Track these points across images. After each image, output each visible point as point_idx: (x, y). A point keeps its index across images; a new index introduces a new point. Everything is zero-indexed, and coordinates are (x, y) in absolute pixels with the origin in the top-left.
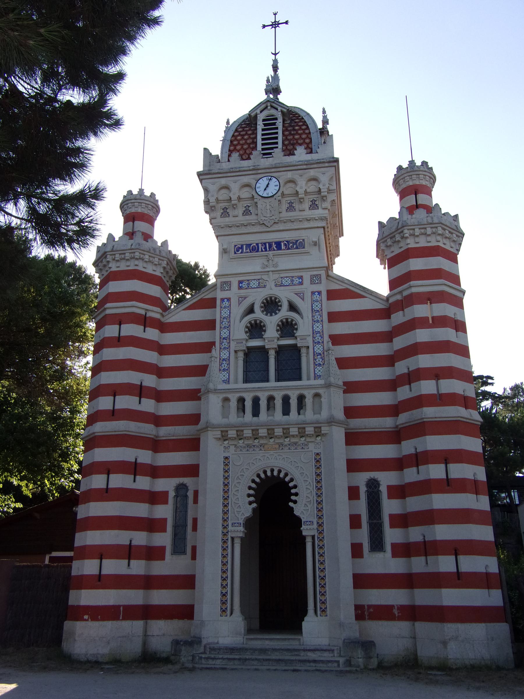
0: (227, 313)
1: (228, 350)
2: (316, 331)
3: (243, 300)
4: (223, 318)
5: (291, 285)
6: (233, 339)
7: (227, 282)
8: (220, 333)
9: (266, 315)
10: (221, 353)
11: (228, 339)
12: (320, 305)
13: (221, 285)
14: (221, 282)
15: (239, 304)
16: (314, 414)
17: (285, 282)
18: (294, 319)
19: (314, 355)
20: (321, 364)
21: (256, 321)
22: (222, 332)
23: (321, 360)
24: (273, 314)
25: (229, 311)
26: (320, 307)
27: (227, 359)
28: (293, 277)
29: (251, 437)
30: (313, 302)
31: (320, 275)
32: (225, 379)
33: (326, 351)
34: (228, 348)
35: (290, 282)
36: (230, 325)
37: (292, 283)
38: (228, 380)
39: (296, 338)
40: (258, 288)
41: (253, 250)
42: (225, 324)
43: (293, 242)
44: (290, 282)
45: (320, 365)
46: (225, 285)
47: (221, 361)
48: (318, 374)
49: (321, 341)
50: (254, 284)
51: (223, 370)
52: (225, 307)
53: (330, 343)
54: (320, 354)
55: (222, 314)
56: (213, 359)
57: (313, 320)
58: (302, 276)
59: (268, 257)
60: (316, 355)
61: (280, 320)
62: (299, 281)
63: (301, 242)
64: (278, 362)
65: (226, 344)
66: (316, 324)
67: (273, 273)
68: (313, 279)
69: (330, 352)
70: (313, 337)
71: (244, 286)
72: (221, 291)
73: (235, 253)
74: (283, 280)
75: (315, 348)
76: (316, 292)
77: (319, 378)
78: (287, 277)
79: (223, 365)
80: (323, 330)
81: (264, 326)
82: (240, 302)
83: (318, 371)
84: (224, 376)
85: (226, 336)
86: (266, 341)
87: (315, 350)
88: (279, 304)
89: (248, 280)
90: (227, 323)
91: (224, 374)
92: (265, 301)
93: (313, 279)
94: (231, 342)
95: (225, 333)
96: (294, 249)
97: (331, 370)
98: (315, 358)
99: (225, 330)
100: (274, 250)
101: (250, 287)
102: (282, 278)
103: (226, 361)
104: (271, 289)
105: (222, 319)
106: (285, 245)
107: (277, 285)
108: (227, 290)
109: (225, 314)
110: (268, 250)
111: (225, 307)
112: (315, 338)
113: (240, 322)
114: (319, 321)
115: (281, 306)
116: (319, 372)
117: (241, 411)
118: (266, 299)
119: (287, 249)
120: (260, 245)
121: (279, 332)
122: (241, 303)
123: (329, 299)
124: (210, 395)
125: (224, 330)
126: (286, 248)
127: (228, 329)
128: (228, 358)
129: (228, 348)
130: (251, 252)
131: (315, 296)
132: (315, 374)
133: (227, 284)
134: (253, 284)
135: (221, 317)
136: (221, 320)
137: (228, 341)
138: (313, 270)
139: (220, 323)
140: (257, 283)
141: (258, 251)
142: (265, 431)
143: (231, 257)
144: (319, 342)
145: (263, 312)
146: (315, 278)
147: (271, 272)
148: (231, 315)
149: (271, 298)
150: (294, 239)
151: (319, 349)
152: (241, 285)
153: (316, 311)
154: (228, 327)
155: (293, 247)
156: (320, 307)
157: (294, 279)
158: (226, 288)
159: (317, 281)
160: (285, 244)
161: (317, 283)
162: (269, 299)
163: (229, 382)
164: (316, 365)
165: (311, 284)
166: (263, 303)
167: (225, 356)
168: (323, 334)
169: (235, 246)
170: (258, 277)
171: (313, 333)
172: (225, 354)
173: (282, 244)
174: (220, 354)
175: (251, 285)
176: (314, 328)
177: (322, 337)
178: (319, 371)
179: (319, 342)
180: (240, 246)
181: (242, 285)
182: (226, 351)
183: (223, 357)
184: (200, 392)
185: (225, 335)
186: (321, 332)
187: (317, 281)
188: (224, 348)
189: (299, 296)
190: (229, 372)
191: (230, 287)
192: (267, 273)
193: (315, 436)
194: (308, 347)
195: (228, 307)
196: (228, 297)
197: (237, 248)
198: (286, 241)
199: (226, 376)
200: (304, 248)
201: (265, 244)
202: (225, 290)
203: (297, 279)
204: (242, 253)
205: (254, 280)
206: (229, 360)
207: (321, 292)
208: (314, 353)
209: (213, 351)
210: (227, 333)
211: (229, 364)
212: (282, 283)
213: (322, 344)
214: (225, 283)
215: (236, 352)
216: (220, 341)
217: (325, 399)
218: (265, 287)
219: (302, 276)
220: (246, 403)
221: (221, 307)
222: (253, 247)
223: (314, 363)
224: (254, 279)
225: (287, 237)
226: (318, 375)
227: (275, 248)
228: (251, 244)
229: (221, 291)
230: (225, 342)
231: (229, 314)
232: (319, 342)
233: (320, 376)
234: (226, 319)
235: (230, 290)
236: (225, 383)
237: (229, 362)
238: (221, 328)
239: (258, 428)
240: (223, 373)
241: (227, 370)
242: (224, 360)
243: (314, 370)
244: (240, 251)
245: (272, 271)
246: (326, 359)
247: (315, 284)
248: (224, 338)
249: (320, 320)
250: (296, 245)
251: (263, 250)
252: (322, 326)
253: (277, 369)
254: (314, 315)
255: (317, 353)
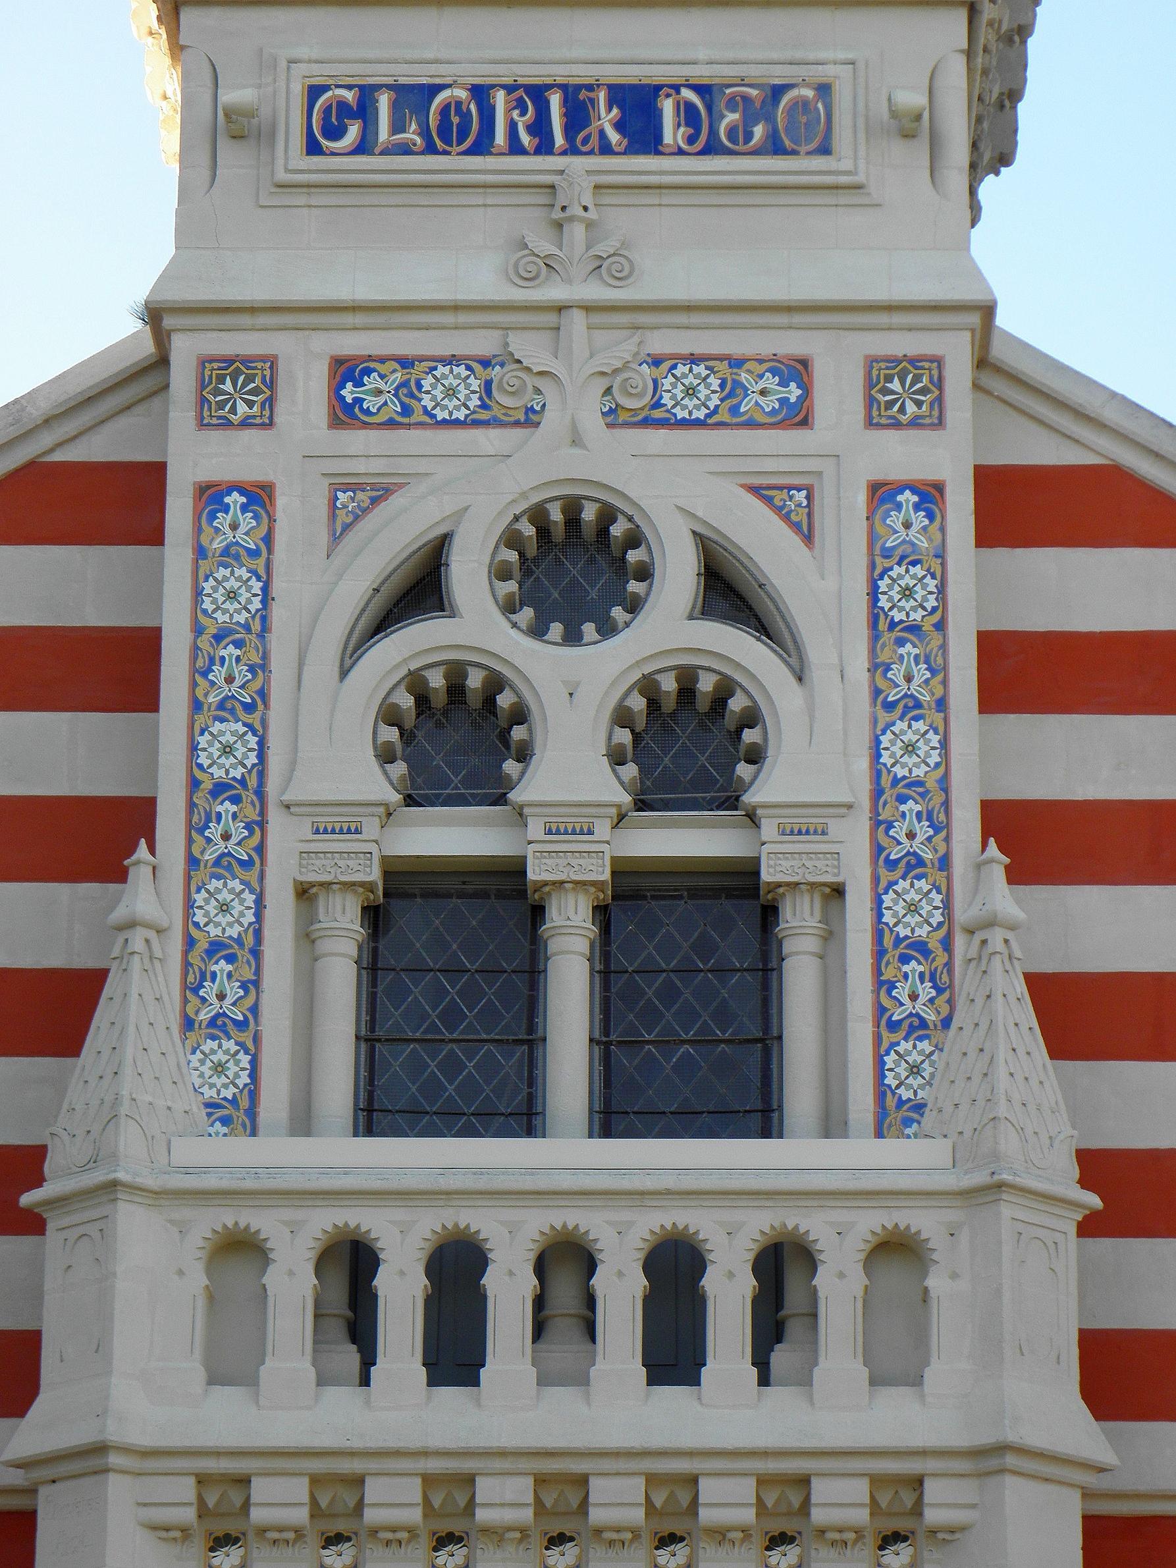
0: (244, 596)
1: (252, 875)
2: (896, 781)
3: (366, 511)
4: (218, 638)
5: (721, 425)
6: (286, 797)
7: (247, 361)
8: (193, 748)
9: (538, 631)
10: (199, 898)
11: (248, 796)
12: (932, 584)
13: (202, 386)
14: (203, 362)
15: (336, 538)
16: (874, 1382)
17: (679, 392)
18: (738, 677)
19: (879, 953)
20: (923, 1024)
21: (456, 673)
22: (203, 741)
23: (926, 991)
24: (589, 630)
25: (257, 586)
26: (931, 602)
27: (239, 941)
28: (737, 363)
29: (412, 1532)
30: (881, 563)
31: (938, 361)
32: (228, 1093)
33: (971, 933)
34: (246, 864)
35: (715, 401)
36: (263, 694)
37: (734, 410)
38: (244, 1103)
39: (752, 818)
40: (477, 423)
41: (447, 141)
42: (230, 680)
43: (746, 99)
44: (715, 401)
45: (918, 1027)
46: (228, 386)
47: (195, 958)
48: (906, 1094)
49: (928, 855)
50: (451, 392)
51: (212, 1023)
52: (230, 555)
53: (998, 874)
54: (921, 948)
55: (208, 605)
56: (138, 944)
57: (876, 692)
58: (805, 363)
59: (561, 200)
60: (892, 955)
61: (636, 675)
62: (782, 392)
63: (803, 105)
64: (606, 986)
65: (238, 831)
66: (900, 726)
67: (597, 318)
68: (886, 391)
69: (996, 937)
70: (876, 823)
71: (371, 403)
72: (202, 424)
73: (313, 148)
74: (667, 383)
75: (888, 899)
76: (902, 487)
77: (907, 1122)
78: (694, 359)
79: (209, 990)
80: (946, 776)
81: (520, 715)
82: (343, 518)
83: (902, 1071)
84: (220, 1068)
85: (237, 773)
86: (535, 829)
87: (888, 918)
88: (633, 556)
89: (406, 363)
90: (241, 673)
91: (220, 1056)
92: (529, 530)
93: (886, 391)
94: (275, 817)
95: (227, 750)
96: (755, 152)
97: (1002, 1072)
98: (888, 974)
99: (229, 730)
100: (606, 149)
101: (418, 416)
102: (656, 362)
103: (230, 959)
104: (576, 441)
105: (204, 642)
106: (689, 115)
107: (623, 417)
108: (245, 423)
109: (231, 606)
110: (559, 140)
111: (230, 555)
112: (890, 826)
113: (344, 673)
114: (918, 705)
115: (644, 573)
116: (915, 1082)
117: (337, 1329)
118: (538, 515)
119: (705, 151)
120: (500, 99)
121: (630, 771)
122: (347, 527)
123: (987, 536)
124: (121, 1206)
125: (217, 727)
126: (691, 140)
127: (255, 719)
128: (249, 940)
129: (246, 864)
130: (431, 149)
131: (896, 520)
132: (881, 1091)
133: (250, 379)
134: (438, 393)
135: (198, 630)
136: (195, 649)
137: (252, 814)
138: (883, 319)
139: (194, 670)
140: (475, 384)
141: (481, 147)
142: (521, 1489)
143: (282, 176)
144: (921, 862)
145: (510, 607)
146: (896, 385)
147: (577, 321)
148: (278, 613)
149: (572, 507)
150: (753, 71)
151: (913, 908)
152: (349, 392)
153: (897, 634)
154: (249, 708)
155: (749, 136)
156: (931, 602)
157: (744, 377)
158: (242, 408)
159: (911, 408)
160: (690, 107)
161: (915, 423)
162: (556, 515)
163: (252, 1113)
164: (893, 1026)
165: (870, 423)
166: (512, 539)
167: (224, 919)
168: (946, 804)
169: (314, 92)
170: (483, 344)
171: (877, 793)
172: (224, 908)
173: (667, 107)
174: (189, 905)
175: (427, 401)
176: (886, 758)
177: (941, 826)
178: (915, 1070)
179: (914, 865)
180: (349, 96)
181: (359, 392)
182: (236, 885)
183: (214, 931)
184: (38, 1180)
185: (228, 761)
186: (931, 784)
187: (911, 408)
188: (217, 862)
189: (778, 510)
190: (257, 1039)
191: (271, 402)
192: (550, 319)
193: (871, 1542)
194: (838, 891)
195: (254, 554)
196: (250, 474)
197: (327, 111)
198: (699, 89)
199: (232, 1069)
200: (825, 150)
201: (538, 93)
202: (227, 424)
203: (770, 382)
204: (362, 148)
205: (451, 361)
206: (256, 953)
207: (939, 487)
208: (878, 935)
209: (140, 875)
210: (240, 751)
211: (253, 985)
212: (657, 405)
213: (940, 878)
214: (231, 365)
215: (304, 893)
216: (191, 806)
217: (954, 1276)
218: (530, 419)
219: (805, 363)
220: (383, 1281)
221: (200, 552)
222: (445, 111)
223: (880, 1010)
224: (447, 352)
225: (702, 55)
226: (901, 1103)
227: (614, 137)
228: (437, 89)
229: (202, 424)
230: (227, 818)
231: (256, 604)
232: (914, 865)
233: (919, 1107)
234: (238, 644)
235: (270, 424)
236: (225, 1121)
237: (258, 971)
238: (196, 705)
239: (468, 1465)
240: (211, 1045)
241: (242, 1025)
242: (215, 948)
243: (879, 1064)
244: (353, 131)
245: (589, 308)
246: (965, 981)
247: (897, 425)
248: (219, 789)
249: (925, 698)
250: (770, 119)
251: (525, 139)
252: (945, 744)
253: (597, 1035)
254: (883, 657)
255: (898, 941)
